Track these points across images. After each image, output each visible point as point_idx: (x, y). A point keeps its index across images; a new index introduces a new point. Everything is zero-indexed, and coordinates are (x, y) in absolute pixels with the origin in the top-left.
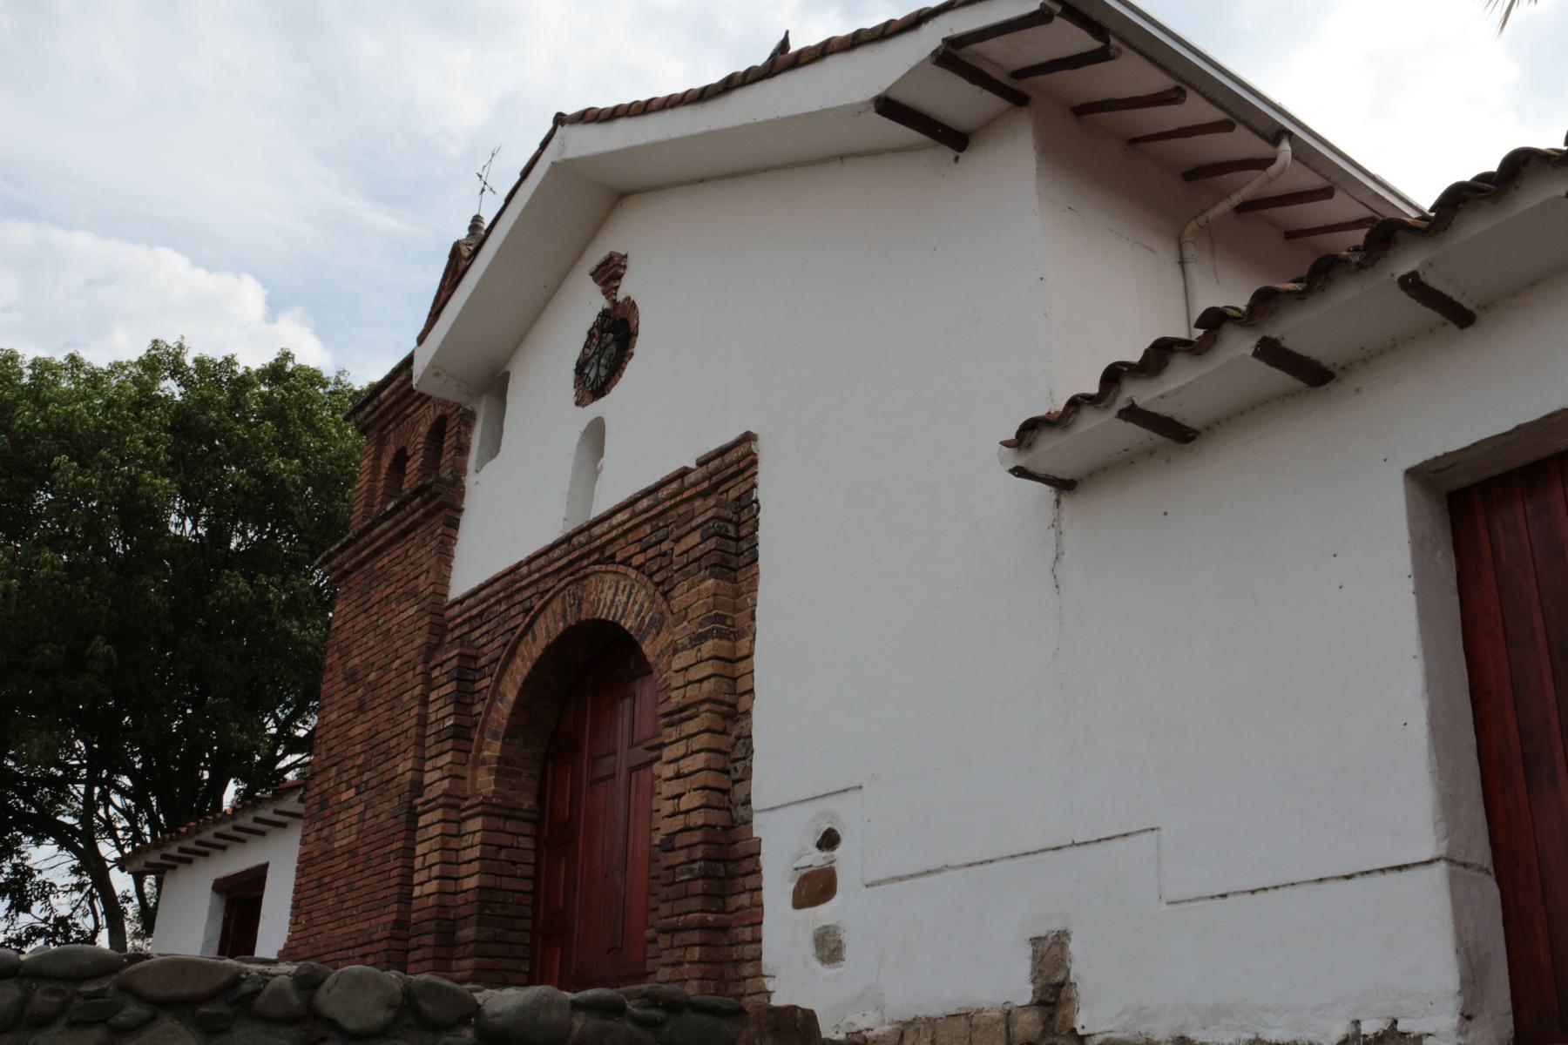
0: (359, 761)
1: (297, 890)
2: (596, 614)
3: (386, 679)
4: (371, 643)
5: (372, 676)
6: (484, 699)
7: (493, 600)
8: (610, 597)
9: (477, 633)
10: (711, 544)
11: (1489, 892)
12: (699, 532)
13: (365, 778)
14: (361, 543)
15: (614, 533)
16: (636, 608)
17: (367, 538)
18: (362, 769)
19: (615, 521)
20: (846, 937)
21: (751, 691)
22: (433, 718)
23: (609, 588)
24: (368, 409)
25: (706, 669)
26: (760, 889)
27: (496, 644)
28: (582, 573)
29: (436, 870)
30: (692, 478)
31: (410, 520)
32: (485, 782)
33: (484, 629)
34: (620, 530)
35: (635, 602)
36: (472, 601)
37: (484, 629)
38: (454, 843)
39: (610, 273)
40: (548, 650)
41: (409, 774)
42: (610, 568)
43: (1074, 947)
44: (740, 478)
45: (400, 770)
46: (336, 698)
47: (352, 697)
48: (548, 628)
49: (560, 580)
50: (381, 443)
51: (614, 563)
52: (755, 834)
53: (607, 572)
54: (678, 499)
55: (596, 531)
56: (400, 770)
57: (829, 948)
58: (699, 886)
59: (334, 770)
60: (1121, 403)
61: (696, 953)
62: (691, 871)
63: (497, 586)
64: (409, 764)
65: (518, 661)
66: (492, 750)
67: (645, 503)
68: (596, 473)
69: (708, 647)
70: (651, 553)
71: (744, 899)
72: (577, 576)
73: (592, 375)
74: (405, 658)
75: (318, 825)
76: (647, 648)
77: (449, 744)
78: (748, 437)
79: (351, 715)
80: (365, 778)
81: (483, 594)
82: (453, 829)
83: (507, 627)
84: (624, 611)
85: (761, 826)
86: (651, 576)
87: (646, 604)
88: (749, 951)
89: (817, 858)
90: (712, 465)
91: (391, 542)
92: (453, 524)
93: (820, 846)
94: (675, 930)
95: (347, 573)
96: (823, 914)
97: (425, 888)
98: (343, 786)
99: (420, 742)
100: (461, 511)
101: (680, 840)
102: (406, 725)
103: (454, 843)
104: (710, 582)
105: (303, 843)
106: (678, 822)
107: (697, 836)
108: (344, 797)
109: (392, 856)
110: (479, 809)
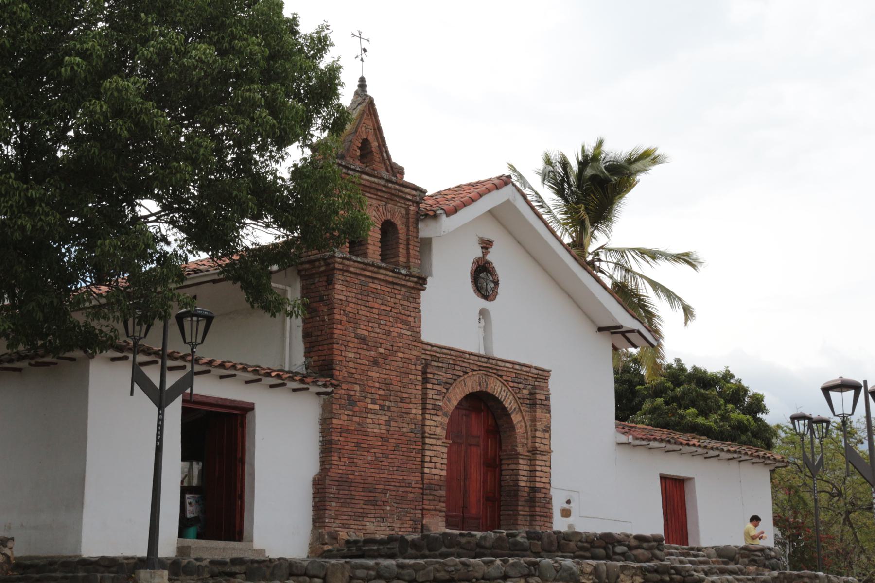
0: (381, 392)
2: (494, 392)
3: (393, 358)
4: (378, 331)
5: (381, 350)
7: (449, 357)
8: (499, 390)
12: (544, 396)
13: (388, 403)
14: (371, 268)
15: (505, 369)
16: (509, 401)
17: (376, 270)
18: (385, 398)
22: (430, 396)
23: (499, 386)
26: (552, 509)
28: (491, 374)
31: (404, 283)
34: (507, 369)
35: (509, 398)
36: (439, 350)
39: (486, 245)
42: (501, 379)
44: (543, 381)
45: (414, 411)
46: (350, 345)
48: (470, 384)
49: (480, 370)
51: (502, 378)
52: (551, 493)
53: (498, 379)
54: (528, 374)
55: (500, 363)
56: (414, 411)
59: (357, 388)
62: (546, 501)
67: (517, 367)
70: (516, 385)
72: (488, 373)
74: (406, 356)
75: (351, 413)
78: (549, 371)
79: (367, 363)
80: (388, 403)
81: (445, 351)
84: (505, 399)
85: (553, 492)
86: (516, 393)
87: (513, 402)
89: (567, 506)
95: (347, 271)
102: (414, 391)
108: (370, 406)
109: (414, 451)
110: (448, 445)
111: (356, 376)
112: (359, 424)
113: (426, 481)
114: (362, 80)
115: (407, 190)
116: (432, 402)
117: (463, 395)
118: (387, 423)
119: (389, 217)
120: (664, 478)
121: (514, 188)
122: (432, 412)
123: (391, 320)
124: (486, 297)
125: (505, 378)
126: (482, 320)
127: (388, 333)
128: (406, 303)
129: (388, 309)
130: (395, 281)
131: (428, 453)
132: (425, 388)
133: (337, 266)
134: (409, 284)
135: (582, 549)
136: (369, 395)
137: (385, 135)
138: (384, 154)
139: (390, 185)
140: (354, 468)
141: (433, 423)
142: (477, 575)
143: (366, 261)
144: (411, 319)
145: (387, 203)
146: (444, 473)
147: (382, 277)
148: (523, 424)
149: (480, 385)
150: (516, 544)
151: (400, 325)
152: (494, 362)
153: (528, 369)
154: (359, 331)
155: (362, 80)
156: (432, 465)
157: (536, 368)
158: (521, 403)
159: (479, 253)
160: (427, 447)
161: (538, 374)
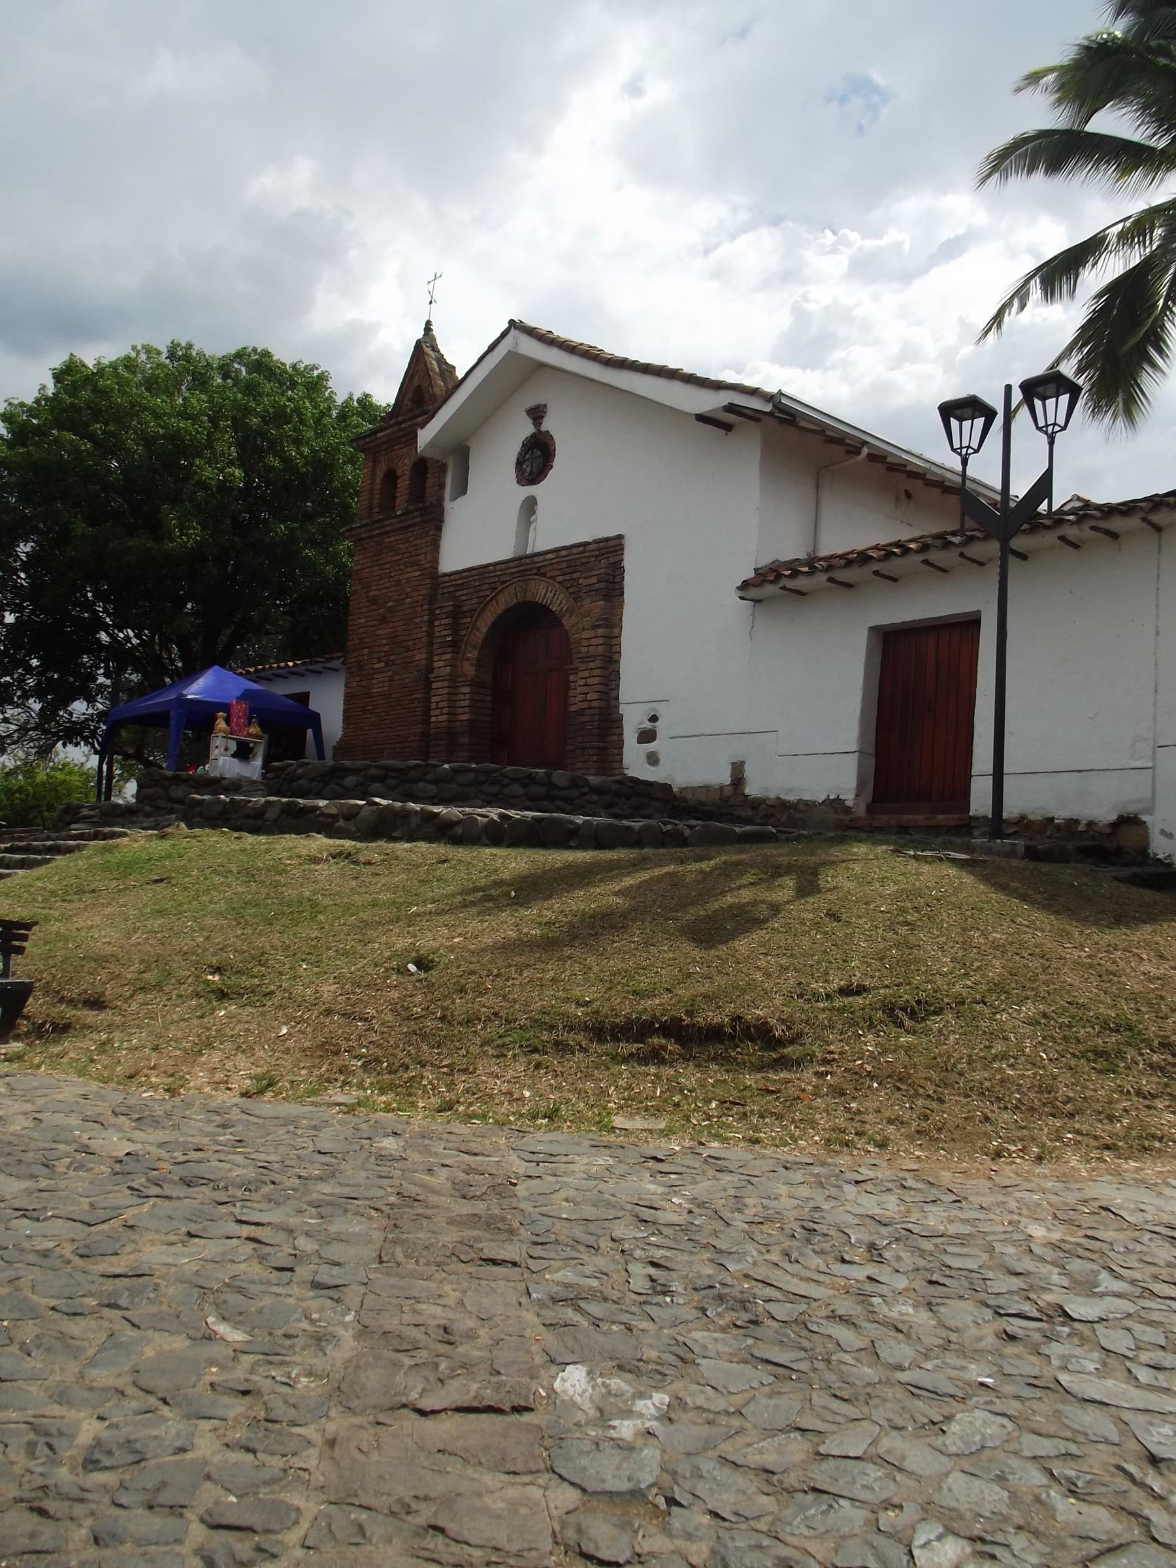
0: (386, 649)
1: (345, 711)
3: (401, 607)
5: (390, 604)
9: (460, 593)
10: (602, 585)
11: (872, 760)
13: (392, 658)
14: (375, 526)
20: (660, 756)
22: (438, 634)
24: (368, 440)
25: (600, 641)
29: (445, 710)
30: (591, 547)
31: (411, 522)
32: (469, 670)
33: (465, 592)
36: (457, 576)
37: (465, 592)
38: (454, 698)
39: (537, 414)
40: (506, 612)
41: (424, 662)
43: (746, 767)
46: (363, 610)
47: (376, 613)
48: (505, 601)
50: (375, 462)
56: (418, 658)
57: (653, 759)
58: (596, 732)
59: (366, 651)
60: (781, 584)
61: (595, 758)
64: (424, 656)
65: (488, 613)
66: (473, 654)
67: (564, 553)
68: (528, 524)
69: (600, 631)
70: (567, 577)
71: (615, 738)
73: (528, 470)
75: (357, 679)
76: (564, 621)
77: (449, 649)
78: (620, 537)
80: (392, 658)
82: (452, 691)
83: (481, 594)
85: (623, 709)
86: (567, 588)
88: (617, 758)
89: (648, 725)
90: (602, 545)
92: (439, 529)
93: (650, 720)
94: (584, 748)
96: (652, 747)
97: (439, 718)
98: (375, 661)
99: (430, 644)
100: (443, 521)
101: (587, 712)
102: (419, 636)
103: (454, 698)
104: (602, 602)
106: (586, 704)
107: (596, 711)
108: (376, 666)
114: (428, 323)
118: (391, 679)
122: (440, 651)
125: (549, 575)
128: (418, 542)
131: (434, 699)
136: (375, 655)
141: (442, 664)
152: (528, 561)
154: (371, 594)
155: (428, 323)
158: (575, 599)
161: (600, 550)
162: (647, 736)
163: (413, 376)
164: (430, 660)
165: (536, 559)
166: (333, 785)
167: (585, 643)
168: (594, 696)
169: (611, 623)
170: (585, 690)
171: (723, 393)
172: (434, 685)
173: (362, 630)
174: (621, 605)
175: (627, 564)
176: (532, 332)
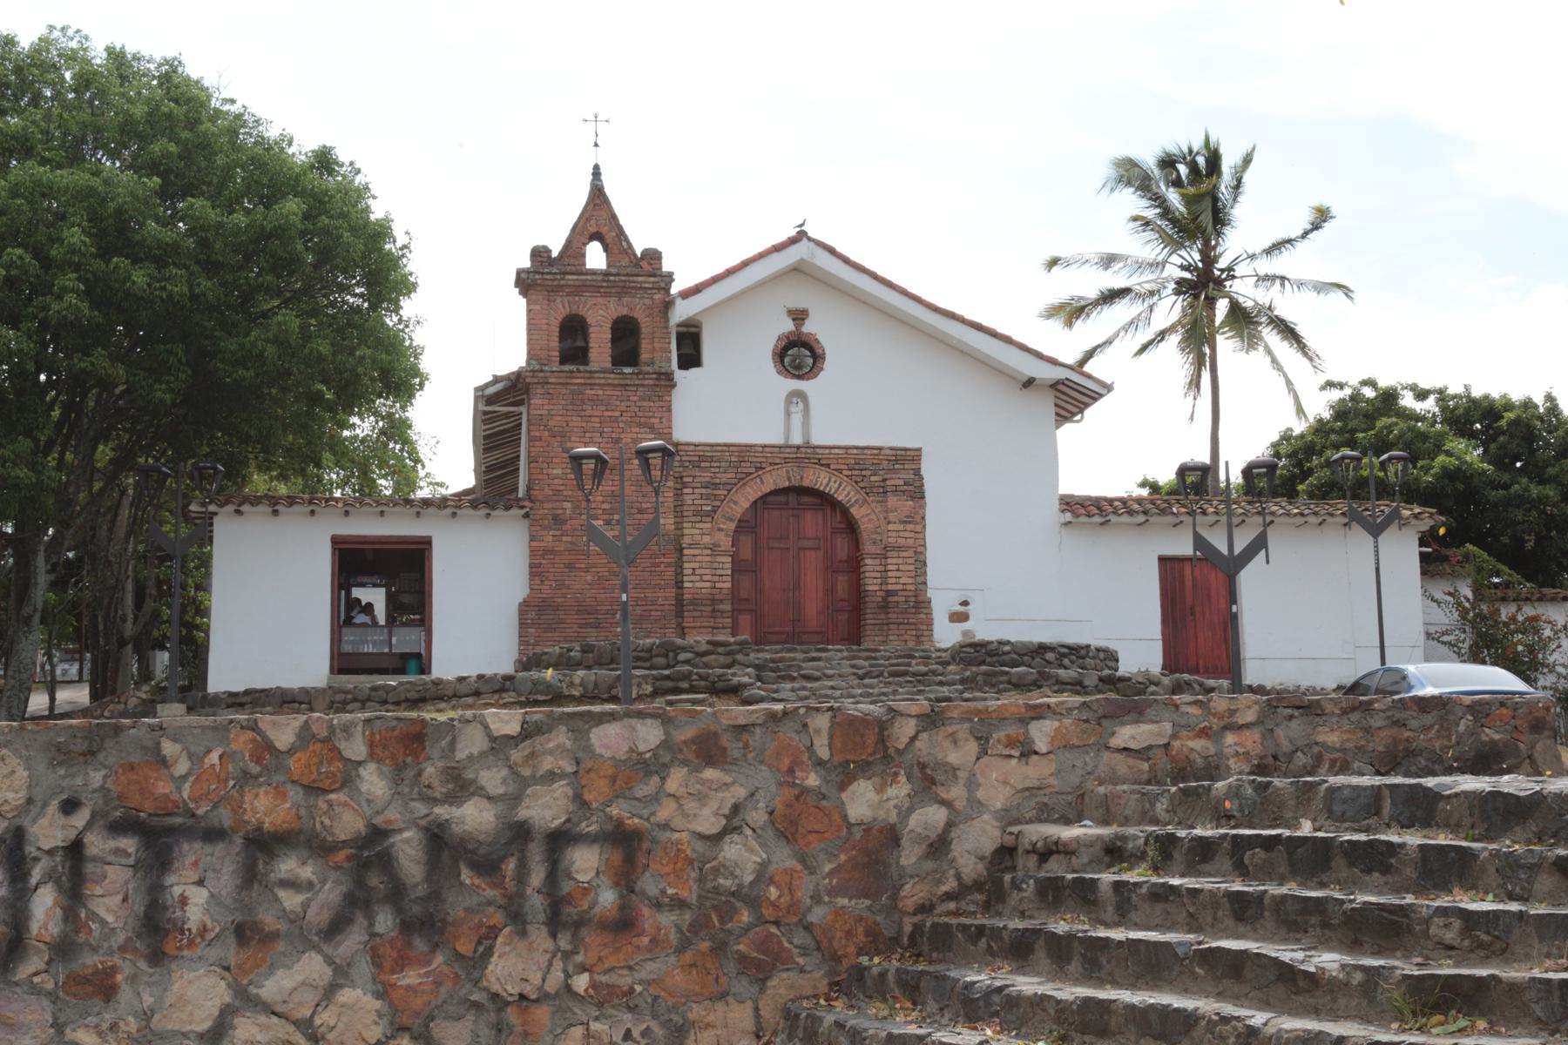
0: (605, 506)
1: (531, 566)
6: (722, 501)
8: (825, 482)
19: (833, 451)
21: (924, 546)
27: (729, 476)
39: (799, 316)
46: (555, 460)
55: (820, 451)
59: (568, 505)
63: (735, 449)
67: (855, 451)
69: (910, 527)
75: (558, 533)
78: (919, 450)
80: (616, 517)
89: (962, 609)
91: (609, 385)
94: (899, 624)
105: (532, 538)
106: (900, 587)
111: (565, 493)
112: (571, 543)
113: (686, 597)
115: (640, 279)
116: (692, 508)
117: (760, 494)
119: (625, 311)
120: (1163, 560)
121: (812, 244)
122: (693, 519)
123: (621, 425)
124: (799, 377)
126: (801, 405)
127: (618, 440)
128: (645, 404)
129: (618, 414)
130: (622, 382)
131: (686, 565)
132: (679, 494)
133: (528, 380)
134: (646, 382)
135: (638, 659)
137: (622, 222)
138: (624, 244)
139: (612, 278)
140: (564, 591)
142: (446, 692)
143: (587, 368)
144: (653, 420)
145: (620, 298)
146: (728, 585)
147: (602, 381)
148: (874, 517)
149: (789, 479)
150: (570, 658)
151: (637, 430)
153: (875, 452)
156: (693, 578)
157: (891, 449)
159: (788, 326)
160: (685, 559)
162: (959, 617)
163: (588, 220)
164: (679, 526)
165: (818, 450)
166: (1038, 660)
167: (894, 534)
168: (911, 581)
169: (916, 520)
170: (898, 574)
171: (1061, 369)
172: (686, 552)
173: (556, 481)
174: (923, 507)
175: (923, 472)
176: (832, 251)
